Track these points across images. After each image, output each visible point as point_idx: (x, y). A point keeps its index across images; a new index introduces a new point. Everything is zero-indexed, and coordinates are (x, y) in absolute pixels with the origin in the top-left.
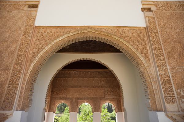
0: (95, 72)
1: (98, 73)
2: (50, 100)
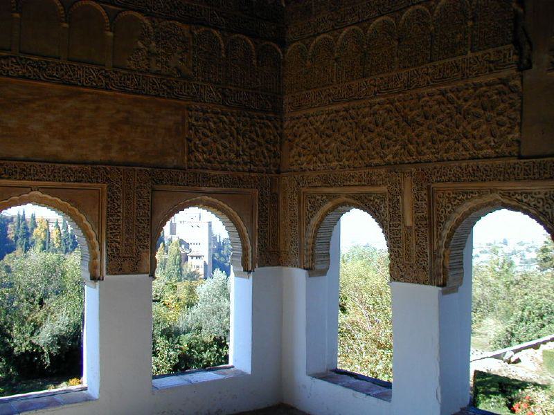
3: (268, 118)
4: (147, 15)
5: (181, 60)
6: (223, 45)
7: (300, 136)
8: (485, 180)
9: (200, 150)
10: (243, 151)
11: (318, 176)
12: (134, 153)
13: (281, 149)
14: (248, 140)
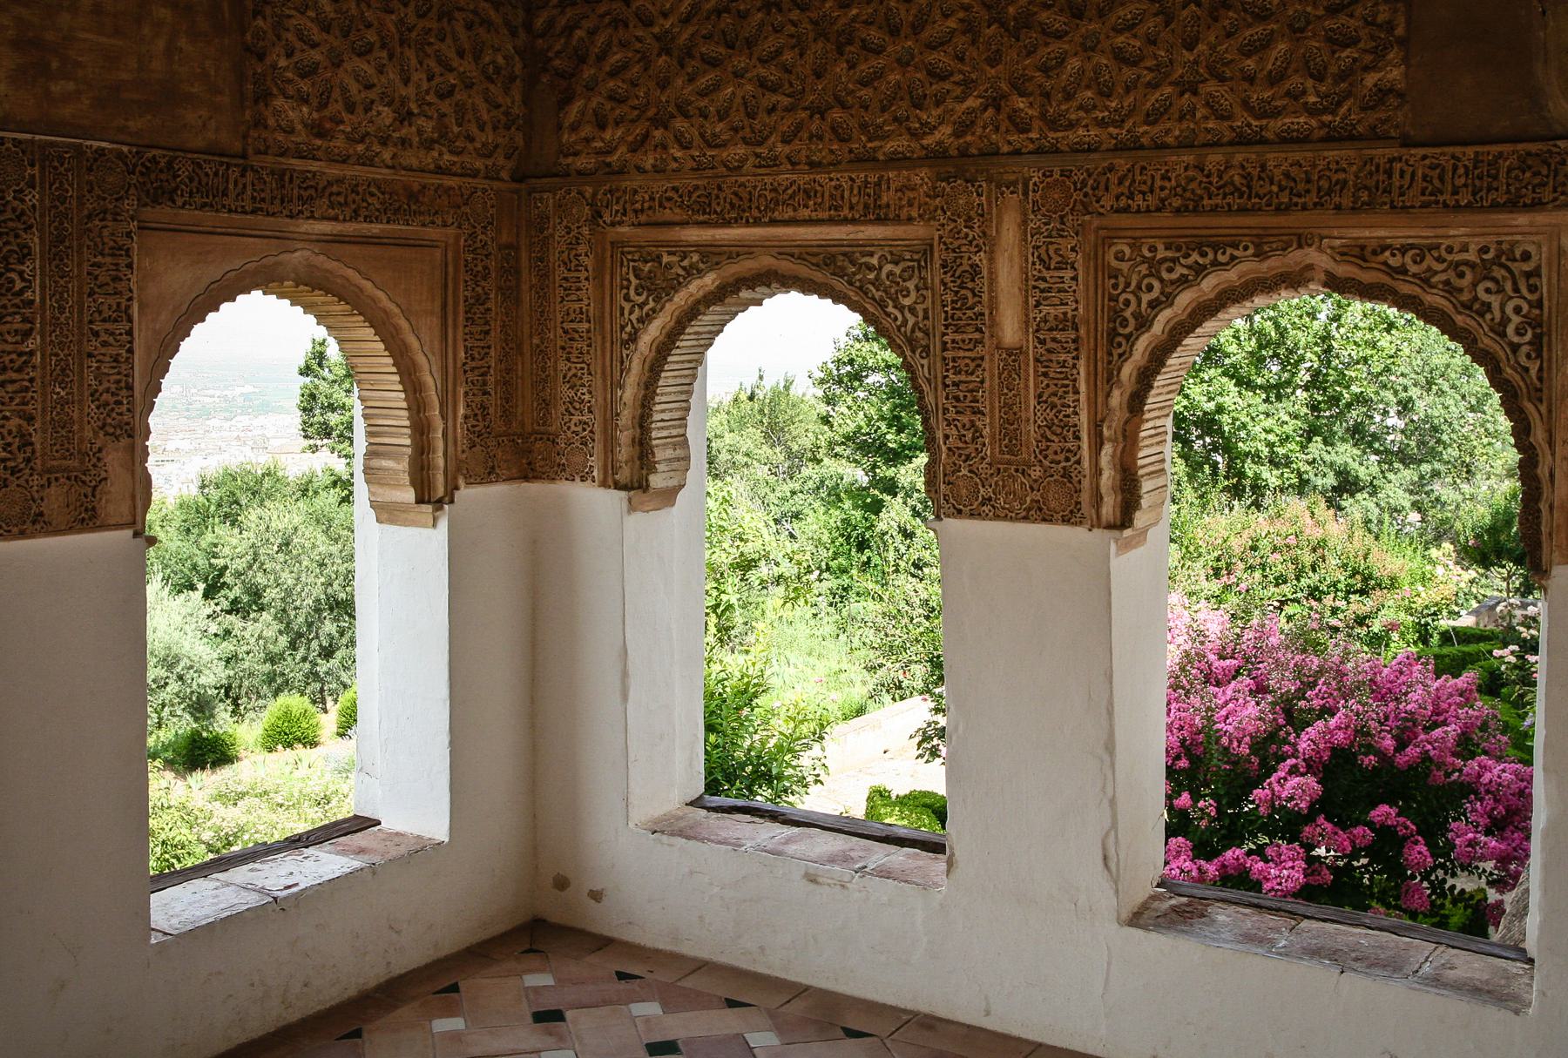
7: (602, 57)
8: (1287, 209)
9: (291, 90)
10: (422, 103)
11: (675, 189)
12: (71, 86)
14: (433, 64)
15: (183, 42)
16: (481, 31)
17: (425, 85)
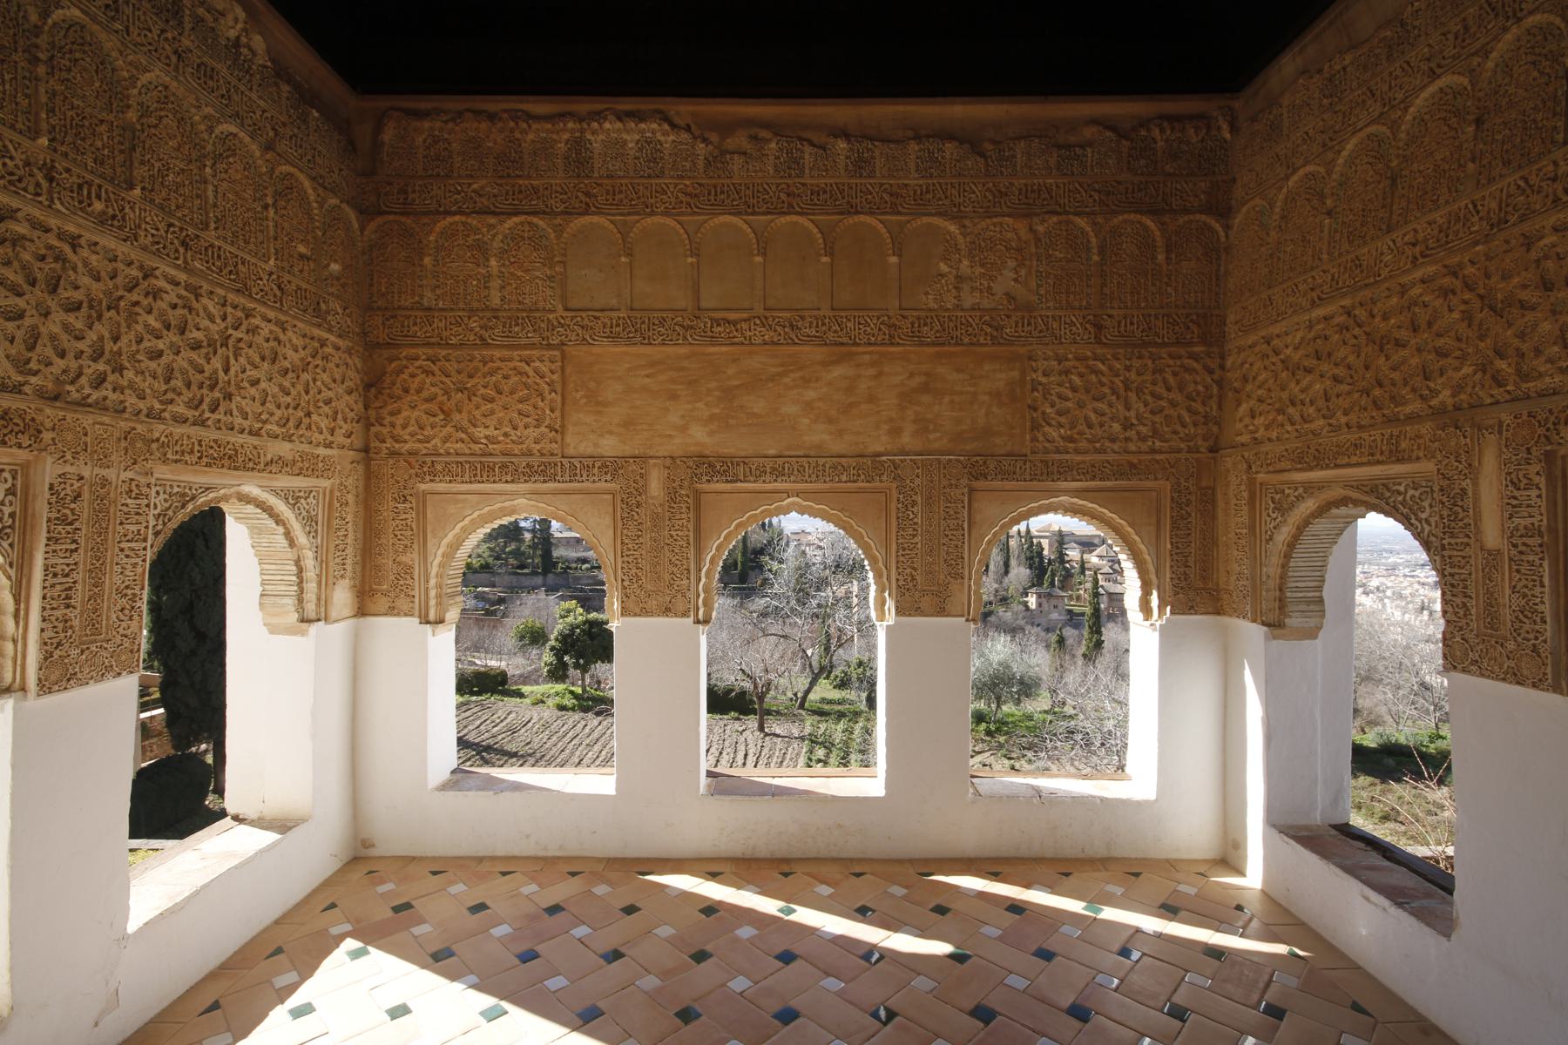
0: (917, 138)
1: (949, 147)
2: (353, 481)
3: (1192, 356)
4: (953, 218)
5: (1016, 280)
6: (1094, 240)
13: (1220, 408)
14: (1149, 398)
15: (994, 409)
16: (1187, 376)
17: (1142, 409)
